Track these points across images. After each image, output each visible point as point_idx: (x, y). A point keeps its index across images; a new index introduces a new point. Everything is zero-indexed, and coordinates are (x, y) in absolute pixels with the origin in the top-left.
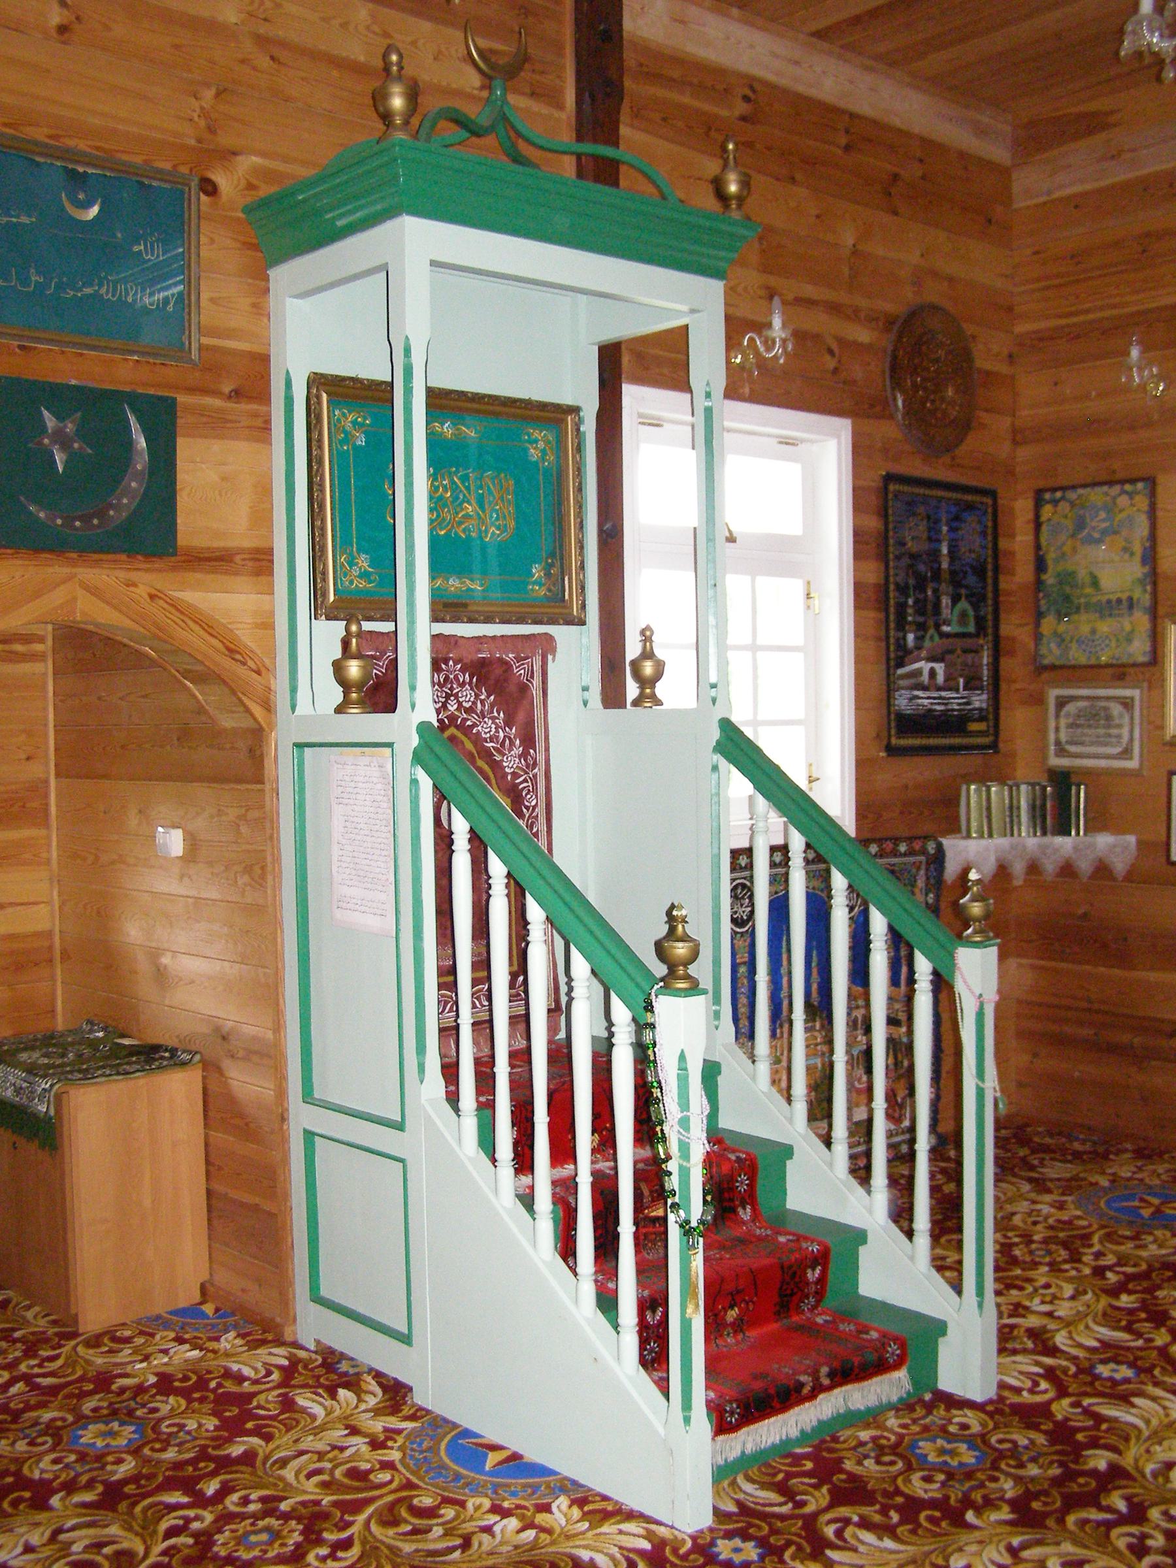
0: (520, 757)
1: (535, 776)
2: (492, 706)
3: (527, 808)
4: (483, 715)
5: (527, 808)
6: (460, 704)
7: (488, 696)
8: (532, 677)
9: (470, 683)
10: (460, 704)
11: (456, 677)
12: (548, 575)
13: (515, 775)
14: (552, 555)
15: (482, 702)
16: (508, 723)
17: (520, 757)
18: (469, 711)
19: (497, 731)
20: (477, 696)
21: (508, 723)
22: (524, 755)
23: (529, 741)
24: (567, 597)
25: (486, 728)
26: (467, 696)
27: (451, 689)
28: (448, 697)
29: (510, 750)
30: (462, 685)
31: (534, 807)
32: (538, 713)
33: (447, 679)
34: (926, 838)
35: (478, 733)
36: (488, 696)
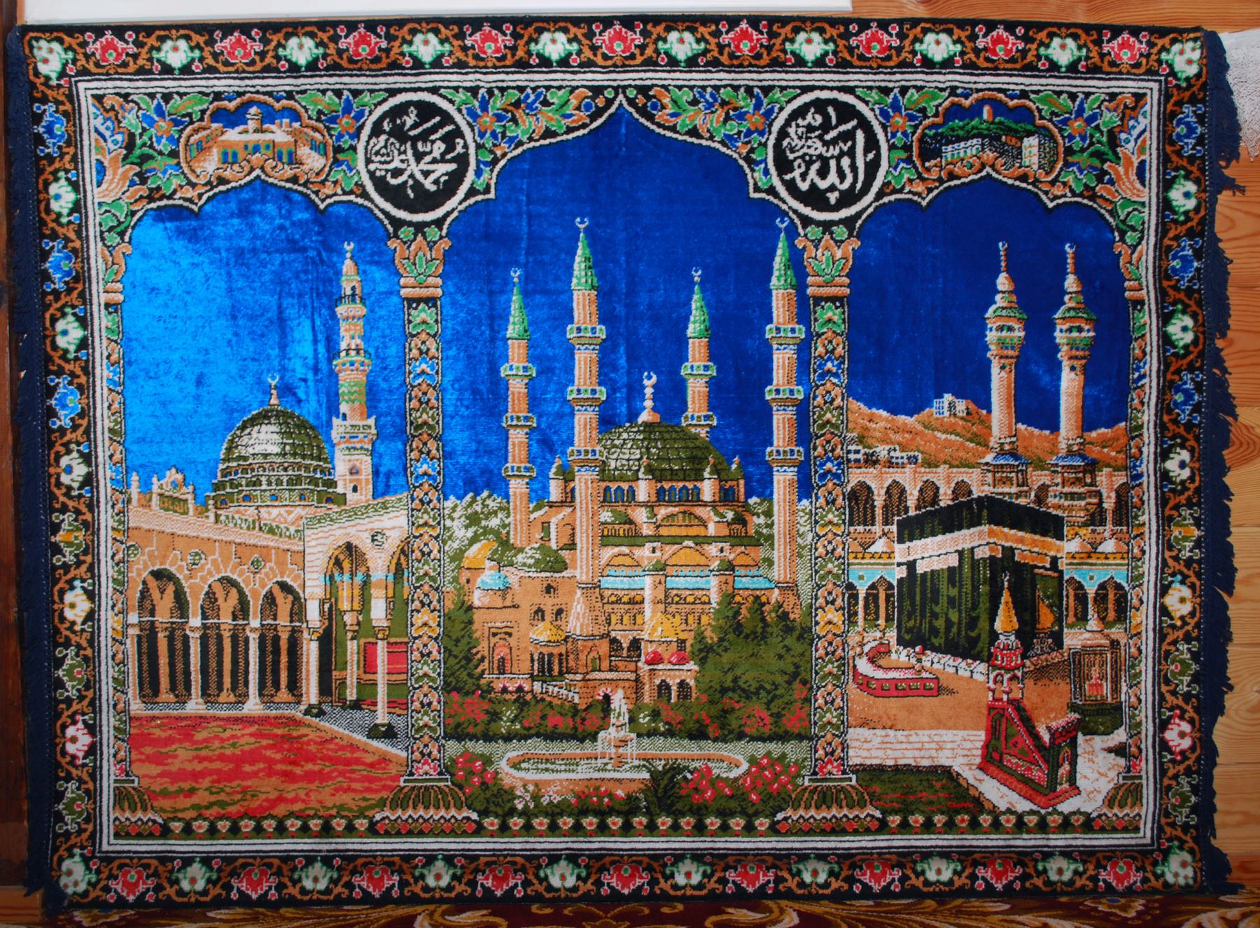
34: (1176, 34)
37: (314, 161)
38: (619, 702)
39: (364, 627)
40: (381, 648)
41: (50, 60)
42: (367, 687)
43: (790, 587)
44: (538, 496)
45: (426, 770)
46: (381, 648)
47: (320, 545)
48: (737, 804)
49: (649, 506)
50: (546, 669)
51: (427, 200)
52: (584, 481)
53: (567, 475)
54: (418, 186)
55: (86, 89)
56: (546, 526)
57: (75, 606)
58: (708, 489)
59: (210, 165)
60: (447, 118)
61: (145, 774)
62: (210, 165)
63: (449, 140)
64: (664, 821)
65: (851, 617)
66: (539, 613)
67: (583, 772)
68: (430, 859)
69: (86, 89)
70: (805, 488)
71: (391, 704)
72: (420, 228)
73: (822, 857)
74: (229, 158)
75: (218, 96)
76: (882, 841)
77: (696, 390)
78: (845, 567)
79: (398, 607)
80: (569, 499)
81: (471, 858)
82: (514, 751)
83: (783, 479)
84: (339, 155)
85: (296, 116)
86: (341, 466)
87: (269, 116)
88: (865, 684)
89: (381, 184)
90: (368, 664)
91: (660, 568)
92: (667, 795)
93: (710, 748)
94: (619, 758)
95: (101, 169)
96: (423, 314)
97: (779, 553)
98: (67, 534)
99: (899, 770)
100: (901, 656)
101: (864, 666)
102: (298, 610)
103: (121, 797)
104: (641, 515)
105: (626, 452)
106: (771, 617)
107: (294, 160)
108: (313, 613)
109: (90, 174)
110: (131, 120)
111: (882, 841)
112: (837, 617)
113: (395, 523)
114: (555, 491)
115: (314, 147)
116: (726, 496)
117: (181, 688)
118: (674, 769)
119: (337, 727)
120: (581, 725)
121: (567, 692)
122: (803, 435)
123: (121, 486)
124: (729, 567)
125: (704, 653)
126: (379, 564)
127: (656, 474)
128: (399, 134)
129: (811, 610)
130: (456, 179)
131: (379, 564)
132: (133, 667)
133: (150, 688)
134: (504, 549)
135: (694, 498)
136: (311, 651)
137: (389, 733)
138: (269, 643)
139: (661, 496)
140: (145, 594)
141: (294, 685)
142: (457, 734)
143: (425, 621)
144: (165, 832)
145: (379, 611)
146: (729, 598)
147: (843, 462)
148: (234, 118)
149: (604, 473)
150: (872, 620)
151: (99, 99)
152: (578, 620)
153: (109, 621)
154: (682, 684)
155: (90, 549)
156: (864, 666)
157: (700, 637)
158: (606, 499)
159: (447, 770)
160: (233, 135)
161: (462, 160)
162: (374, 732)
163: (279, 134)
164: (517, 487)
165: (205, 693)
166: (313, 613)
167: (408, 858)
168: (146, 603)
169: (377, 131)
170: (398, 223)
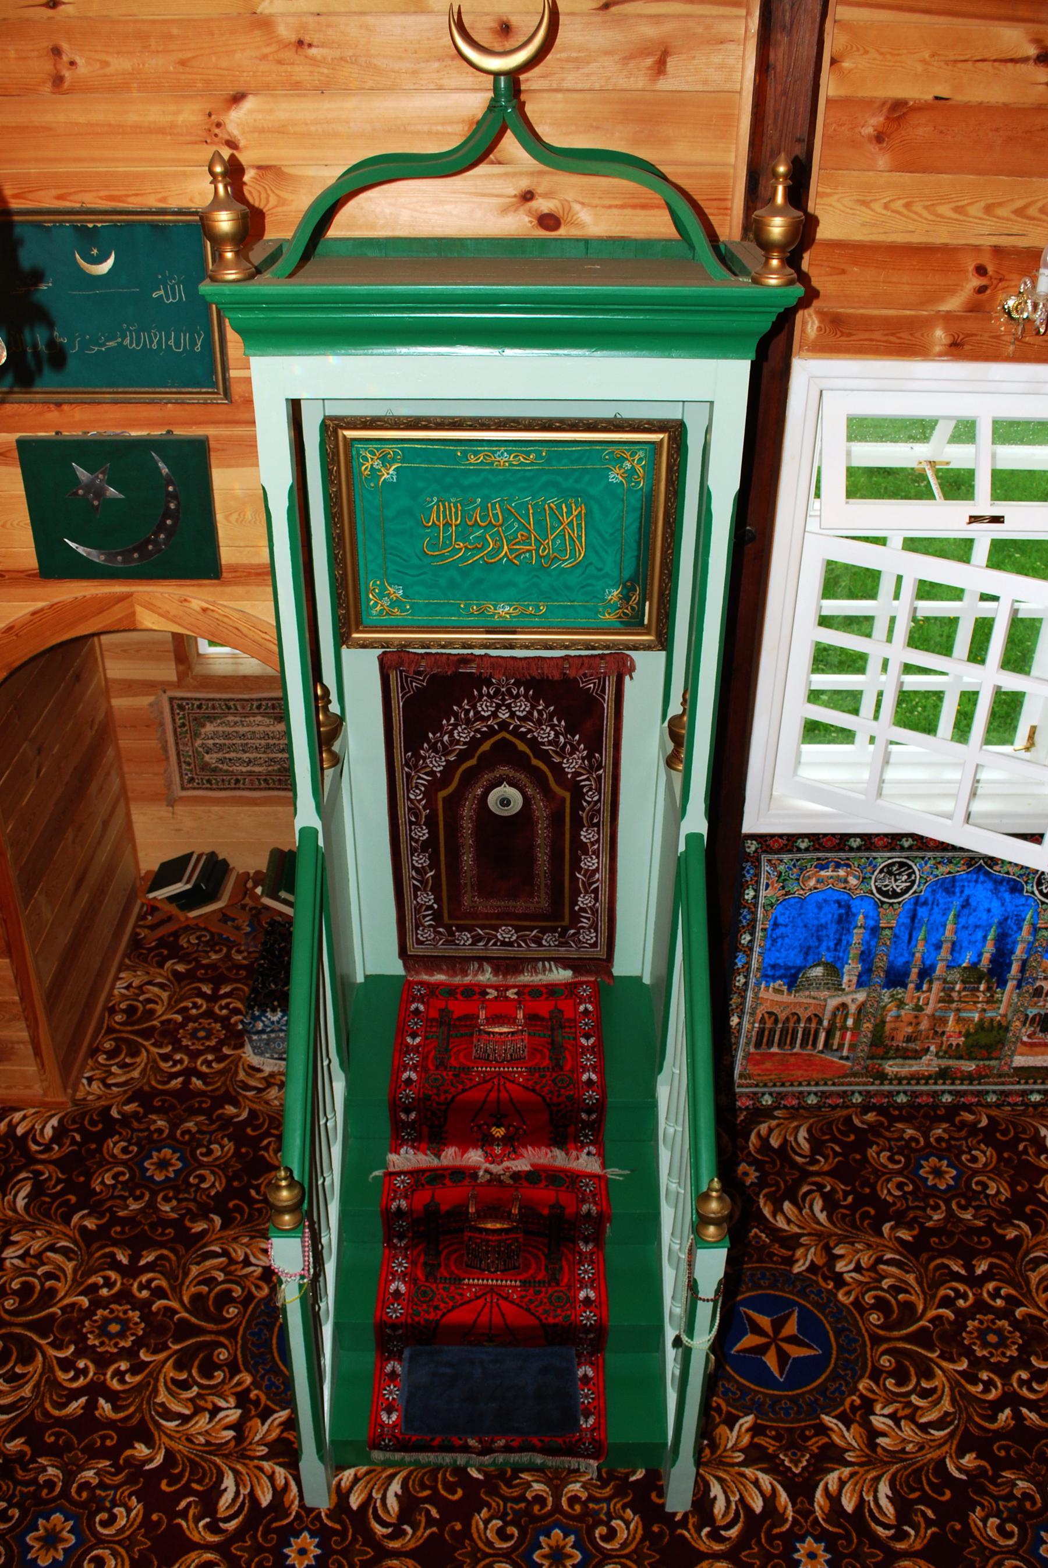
0: (583, 759)
1: (599, 777)
2: (551, 716)
3: (589, 803)
4: (539, 723)
5: (589, 803)
6: (513, 715)
7: (547, 707)
8: (603, 691)
9: (526, 696)
10: (513, 715)
11: (509, 691)
12: (626, 598)
13: (577, 774)
14: (634, 580)
15: (540, 712)
16: (570, 730)
17: (583, 759)
18: (519, 718)
19: (557, 736)
20: (533, 707)
21: (570, 730)
22: (589, 757)
23: (594, 744)
24: (646, 622)
25: (545, 735)
26: (522, 707)
27: (504, 700)
28: (498, 707)
29: (571, 754)
30: (518, 696)
31: (596, 802)
32: (609, 724)
33: (497, 692)
35: (535, 738)
36: (547, 707)
37: (853, 881)
38: (933, 1048)
39: (844, 1028)
40: (849, 1034)
41: (752, 847)
42: (841, 1047)
43: (1005, 1016)
44: (919, 987)
45: (857, 1068)
46: (849, 1034)
47: (833, 1003)
48: (969, 1078)
49: (959, 992)
50: (909, 1039)
51: (895, 895)
52: (936, 986)
53: (931, 982)
54: (894, 890)
55: (764, 857)
56: (919, 998)
57: (734, 1021)
58: (982, 987)
59: (812, 883)
60: (910, 867)
61: (751, 1069)
62: (812, 883)
63: (909, 875)
64: (940, 1081)
65: (1024, 1024)
66: (911, 1024)
67: (914, 1069)
68: (853, 1092)
69: (764, 857)
70: (1019, 986)
71: (849, 1050)
72: (891, 904)
73: (994, 1092)
74: (818, 881)
75: (818, 859)
76: (1017, 1087)
77: (986, 956)
78: (1026, 1008)
79: (858, 1022)
80: (930, 990)
81: (868, 1092)
82: (891, 1062)
83: (1011, 984)
84: (864, 880)
85: (848, 866)
86: (845, 979)
87: (838, 866)
88: (1024, 1043)
89: (879, 890)
90: (843, 1037)
91: (958, 1010)
92: (944, 1074)
93: (962, 1062)
94: (929, 1064)
95: (767, 886)
96: (887, 932)
97: (1003, 1006)
98: (735, 1000)
99: (1029, 1068)
100: (1040, 1035)
101: (1025, 1039)
102: (820, 1022)
103: (741, 1076)
104: (955, 995)
105: (955, 975)
106: (995, 1024)
107: (846, 881)
108: (825, 1023)
109: (762, 887)
110: (781, 868)
111: (1017, 1087)
112: (1018, 1023)
113: (861, 996)
114: (925, 987)
115: (855, 876)
116: (989, 989)
117: (770, 1044)
118: (948, 1068)
119: (828, 1057)
120: (917, 1055)
121: (916, 1046)
122: (1023, 969)
123: (758, 984)
124: (984, 1010)
125: (968, 1035)
126: (853, 1008)
127: (963, 982)
128: (890, 873)
129: (1009, 1023)
130: (908, 888)
131: (853, 1008)
132: (754, 1039)
133: (758, 1044)
134: (901, 1004)
135: (978, 990)
136: (822, 1036)
137: (847, 1058)
138: (806, 1032)
139: (964, 989)
140: (763, 1018)
141: (814, 1045)
142: (872, 1058)
143: (867, 1026)
144: (757, 1086)
145: (850, 1022)
146: (981, 1020)
147: (1035, 979)
148: (823, 868)
149: (945, 981)
150: (1031, 1025)
151: (769, 861)
152: (925, 1024)
153: (746, 1025)
154: (958, 1045)
155: (743, 1004)
156: (1025, 1039)
157: (968, 1030)
158: (943, 990)
159: (866, 1068)
160: (822, 873)
161: (913, 882)
162: (842, 1058)
163: (841, 873)
164: (911, 986)
165: (779, 1046)
166: (825, 1023)
167: (845, 1092)
168: (762, 1020)
169: (881, 871)
170: (883, 903)
